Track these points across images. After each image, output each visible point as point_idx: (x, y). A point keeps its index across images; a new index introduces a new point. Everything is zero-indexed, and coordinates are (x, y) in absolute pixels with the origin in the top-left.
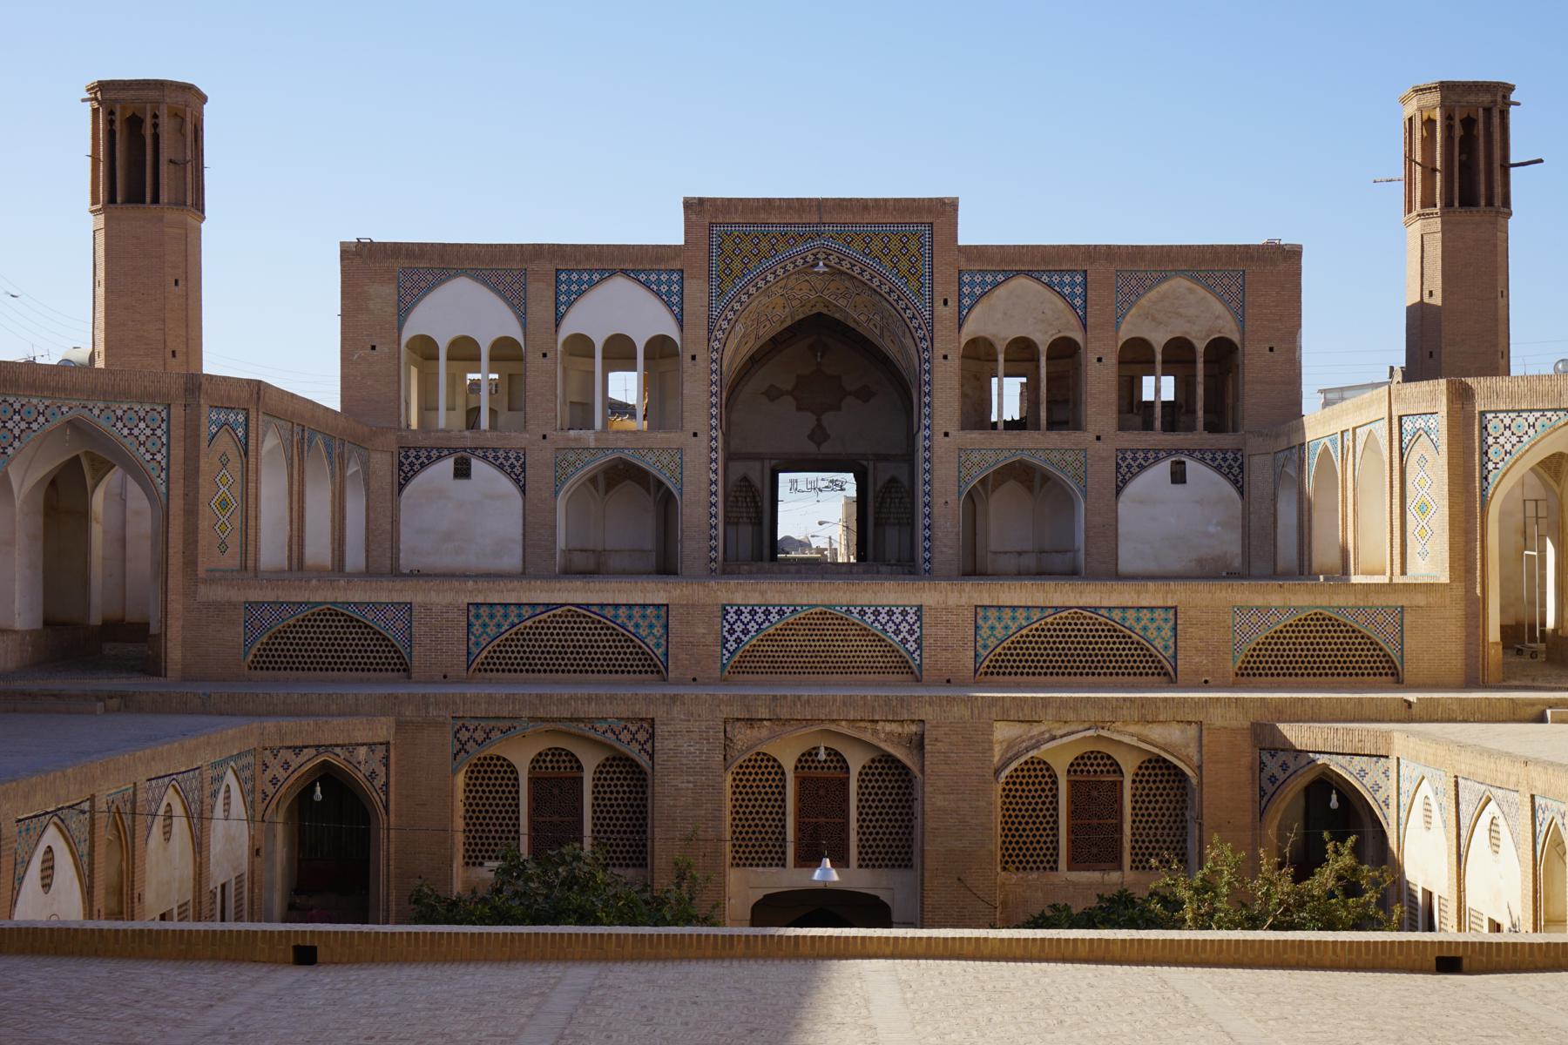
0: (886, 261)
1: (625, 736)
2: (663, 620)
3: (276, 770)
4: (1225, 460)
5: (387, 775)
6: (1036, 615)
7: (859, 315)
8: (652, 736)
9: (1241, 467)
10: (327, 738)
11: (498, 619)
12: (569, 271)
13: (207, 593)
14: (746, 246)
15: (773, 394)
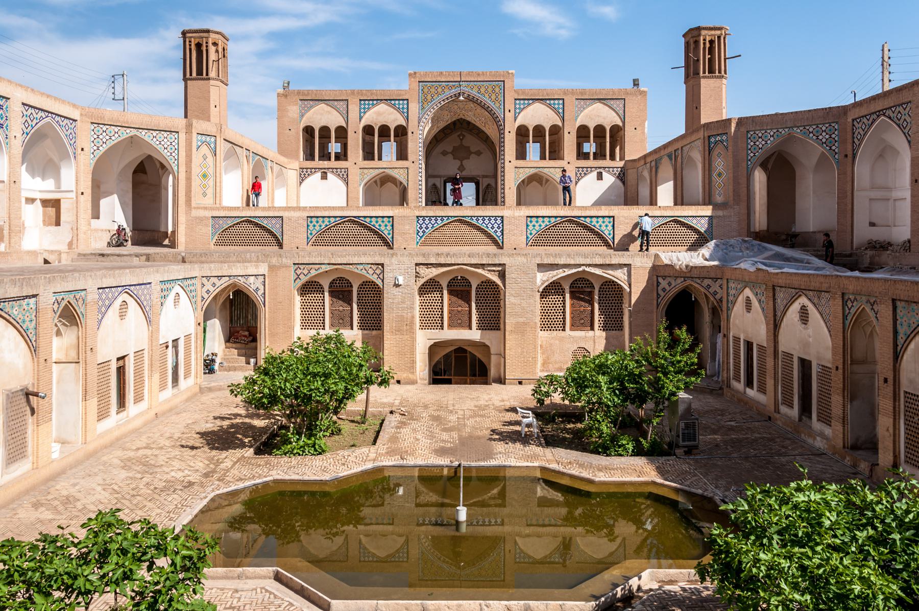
0: (487, 95)
1: (371, 271)
3: (208, 286)
6: (553, 220)
8: (383, 272)
10: (235, 272)
13: (195, 213)
14: (433, 90)
15: (444, 153)
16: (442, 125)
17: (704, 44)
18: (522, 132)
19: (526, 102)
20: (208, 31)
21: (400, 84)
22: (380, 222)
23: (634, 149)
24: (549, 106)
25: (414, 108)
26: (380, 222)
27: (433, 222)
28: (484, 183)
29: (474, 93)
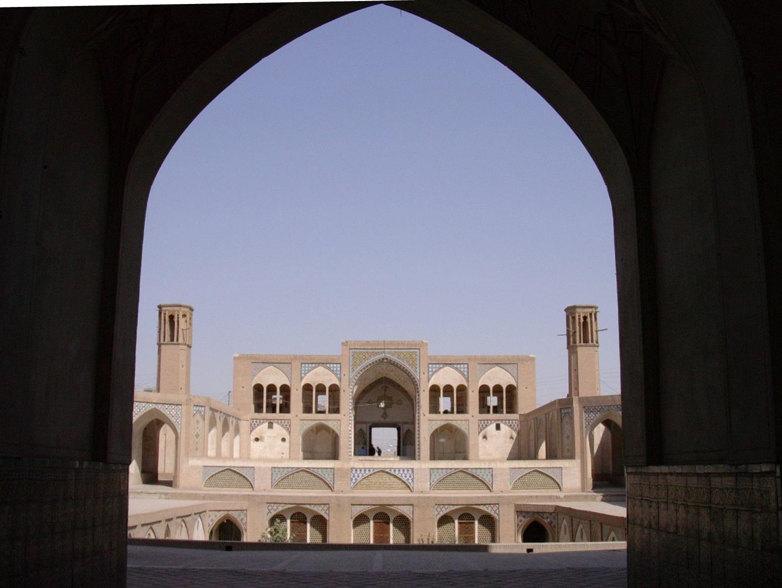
2: (332, 473)
4: (512, 423)
5: (246, 520)
6: (449, 471)
12: (304, 363)
16: (368, 382)
17: (579, 319)
18: (434, 390)
19: (438, 366)
20: (180, 306)
21: (334, 350)
22: (324, 472)
23: (531, 400)
24: (457, 369)
25: (345, 371)
26: (324, 472)
27: (363, 472)
28: (405, 428)
29: (395, 358)
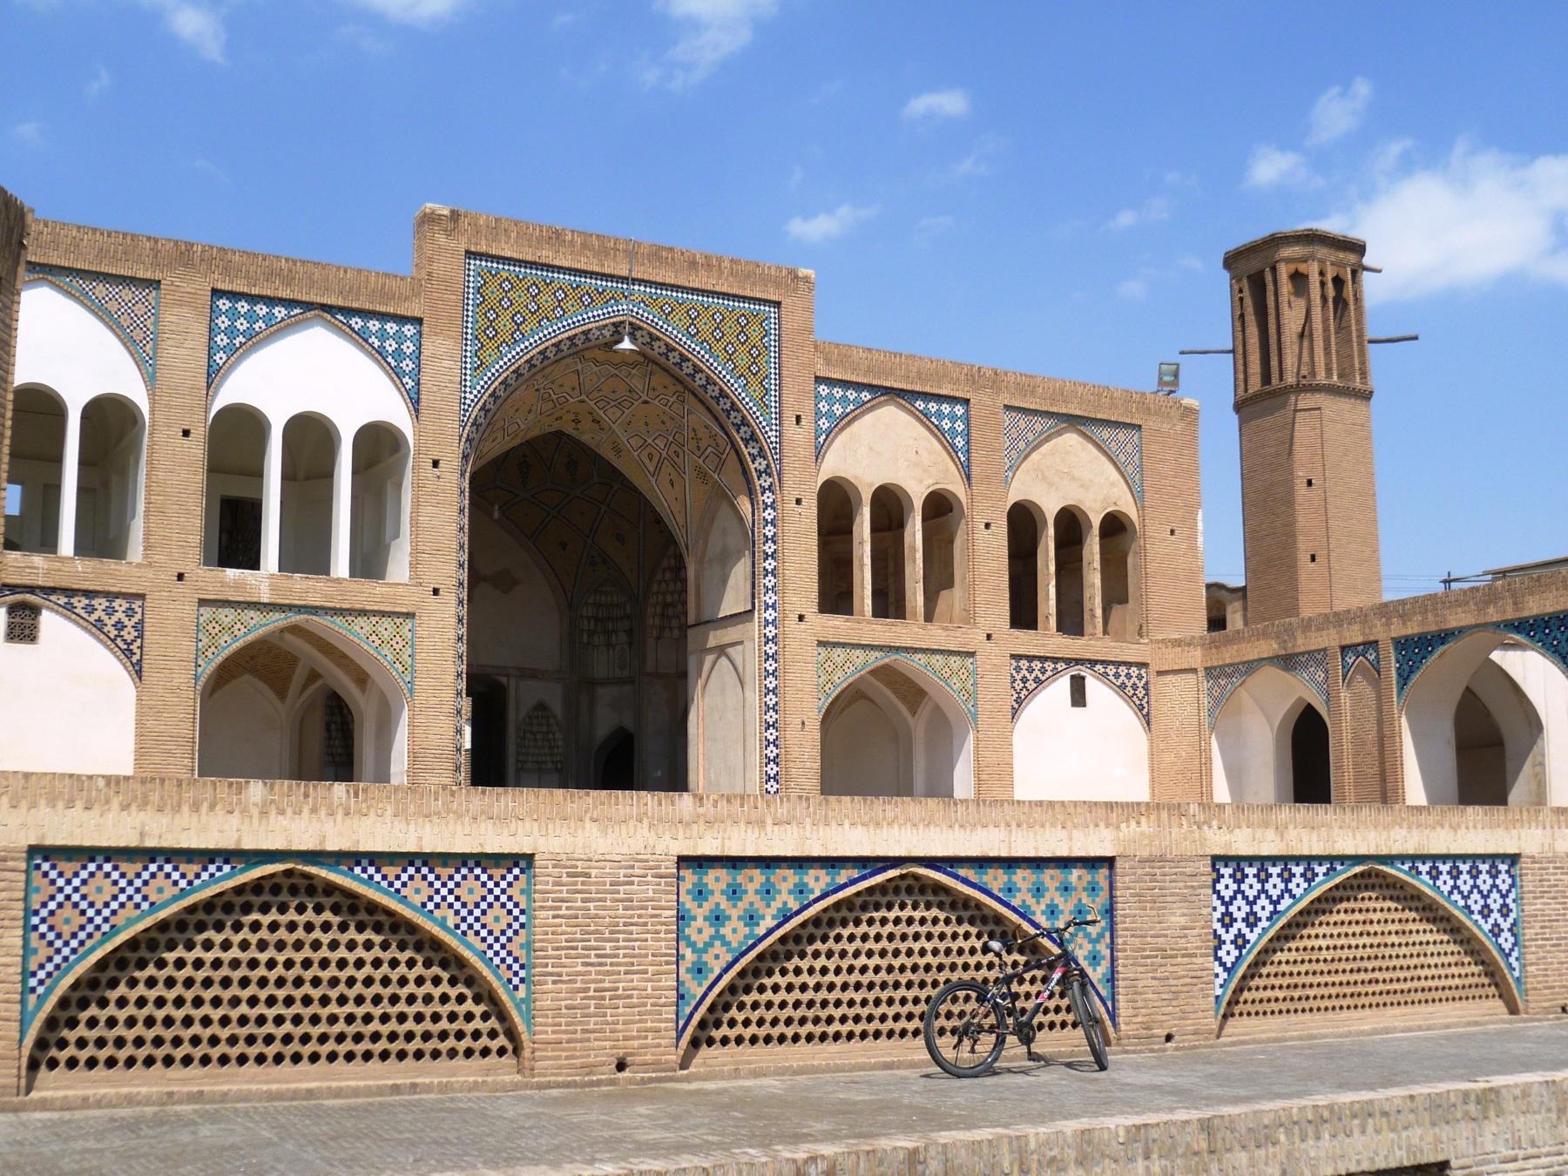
7: (630, 439)
9: (1146, 687)
11: (751, 897)
12: (235, 296)
14: (519, 296)
19: (851, 394)
24: (924, 418)
27: (1275, 886)
29: (673, 331)
